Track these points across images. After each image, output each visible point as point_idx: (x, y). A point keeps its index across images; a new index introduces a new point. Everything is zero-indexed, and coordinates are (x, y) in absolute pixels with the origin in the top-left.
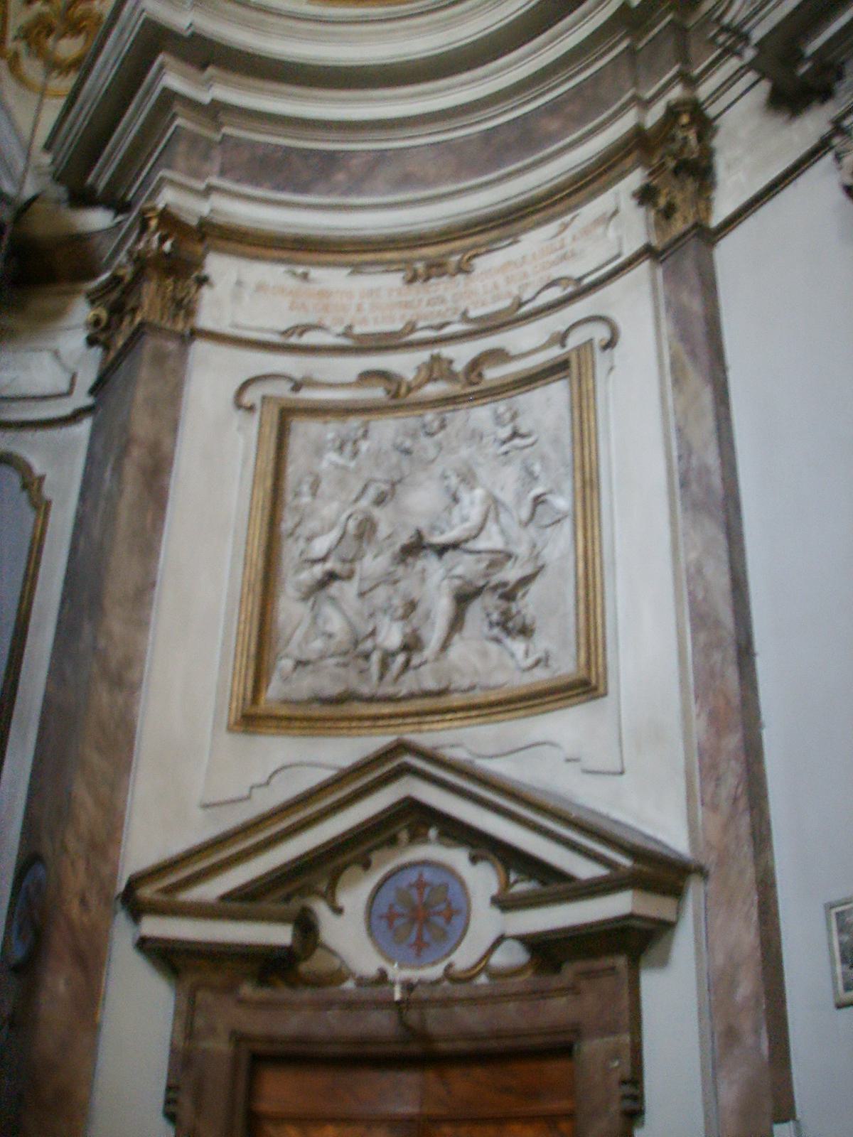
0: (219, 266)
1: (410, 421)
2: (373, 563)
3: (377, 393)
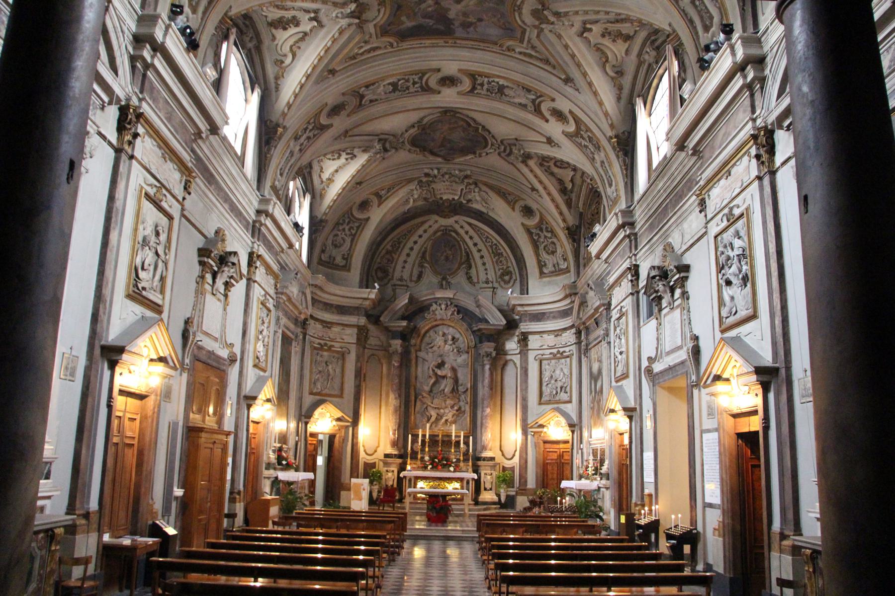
0: (530, 337)
1: (557, 361)
2: (553, 382)
3: (551, 356)
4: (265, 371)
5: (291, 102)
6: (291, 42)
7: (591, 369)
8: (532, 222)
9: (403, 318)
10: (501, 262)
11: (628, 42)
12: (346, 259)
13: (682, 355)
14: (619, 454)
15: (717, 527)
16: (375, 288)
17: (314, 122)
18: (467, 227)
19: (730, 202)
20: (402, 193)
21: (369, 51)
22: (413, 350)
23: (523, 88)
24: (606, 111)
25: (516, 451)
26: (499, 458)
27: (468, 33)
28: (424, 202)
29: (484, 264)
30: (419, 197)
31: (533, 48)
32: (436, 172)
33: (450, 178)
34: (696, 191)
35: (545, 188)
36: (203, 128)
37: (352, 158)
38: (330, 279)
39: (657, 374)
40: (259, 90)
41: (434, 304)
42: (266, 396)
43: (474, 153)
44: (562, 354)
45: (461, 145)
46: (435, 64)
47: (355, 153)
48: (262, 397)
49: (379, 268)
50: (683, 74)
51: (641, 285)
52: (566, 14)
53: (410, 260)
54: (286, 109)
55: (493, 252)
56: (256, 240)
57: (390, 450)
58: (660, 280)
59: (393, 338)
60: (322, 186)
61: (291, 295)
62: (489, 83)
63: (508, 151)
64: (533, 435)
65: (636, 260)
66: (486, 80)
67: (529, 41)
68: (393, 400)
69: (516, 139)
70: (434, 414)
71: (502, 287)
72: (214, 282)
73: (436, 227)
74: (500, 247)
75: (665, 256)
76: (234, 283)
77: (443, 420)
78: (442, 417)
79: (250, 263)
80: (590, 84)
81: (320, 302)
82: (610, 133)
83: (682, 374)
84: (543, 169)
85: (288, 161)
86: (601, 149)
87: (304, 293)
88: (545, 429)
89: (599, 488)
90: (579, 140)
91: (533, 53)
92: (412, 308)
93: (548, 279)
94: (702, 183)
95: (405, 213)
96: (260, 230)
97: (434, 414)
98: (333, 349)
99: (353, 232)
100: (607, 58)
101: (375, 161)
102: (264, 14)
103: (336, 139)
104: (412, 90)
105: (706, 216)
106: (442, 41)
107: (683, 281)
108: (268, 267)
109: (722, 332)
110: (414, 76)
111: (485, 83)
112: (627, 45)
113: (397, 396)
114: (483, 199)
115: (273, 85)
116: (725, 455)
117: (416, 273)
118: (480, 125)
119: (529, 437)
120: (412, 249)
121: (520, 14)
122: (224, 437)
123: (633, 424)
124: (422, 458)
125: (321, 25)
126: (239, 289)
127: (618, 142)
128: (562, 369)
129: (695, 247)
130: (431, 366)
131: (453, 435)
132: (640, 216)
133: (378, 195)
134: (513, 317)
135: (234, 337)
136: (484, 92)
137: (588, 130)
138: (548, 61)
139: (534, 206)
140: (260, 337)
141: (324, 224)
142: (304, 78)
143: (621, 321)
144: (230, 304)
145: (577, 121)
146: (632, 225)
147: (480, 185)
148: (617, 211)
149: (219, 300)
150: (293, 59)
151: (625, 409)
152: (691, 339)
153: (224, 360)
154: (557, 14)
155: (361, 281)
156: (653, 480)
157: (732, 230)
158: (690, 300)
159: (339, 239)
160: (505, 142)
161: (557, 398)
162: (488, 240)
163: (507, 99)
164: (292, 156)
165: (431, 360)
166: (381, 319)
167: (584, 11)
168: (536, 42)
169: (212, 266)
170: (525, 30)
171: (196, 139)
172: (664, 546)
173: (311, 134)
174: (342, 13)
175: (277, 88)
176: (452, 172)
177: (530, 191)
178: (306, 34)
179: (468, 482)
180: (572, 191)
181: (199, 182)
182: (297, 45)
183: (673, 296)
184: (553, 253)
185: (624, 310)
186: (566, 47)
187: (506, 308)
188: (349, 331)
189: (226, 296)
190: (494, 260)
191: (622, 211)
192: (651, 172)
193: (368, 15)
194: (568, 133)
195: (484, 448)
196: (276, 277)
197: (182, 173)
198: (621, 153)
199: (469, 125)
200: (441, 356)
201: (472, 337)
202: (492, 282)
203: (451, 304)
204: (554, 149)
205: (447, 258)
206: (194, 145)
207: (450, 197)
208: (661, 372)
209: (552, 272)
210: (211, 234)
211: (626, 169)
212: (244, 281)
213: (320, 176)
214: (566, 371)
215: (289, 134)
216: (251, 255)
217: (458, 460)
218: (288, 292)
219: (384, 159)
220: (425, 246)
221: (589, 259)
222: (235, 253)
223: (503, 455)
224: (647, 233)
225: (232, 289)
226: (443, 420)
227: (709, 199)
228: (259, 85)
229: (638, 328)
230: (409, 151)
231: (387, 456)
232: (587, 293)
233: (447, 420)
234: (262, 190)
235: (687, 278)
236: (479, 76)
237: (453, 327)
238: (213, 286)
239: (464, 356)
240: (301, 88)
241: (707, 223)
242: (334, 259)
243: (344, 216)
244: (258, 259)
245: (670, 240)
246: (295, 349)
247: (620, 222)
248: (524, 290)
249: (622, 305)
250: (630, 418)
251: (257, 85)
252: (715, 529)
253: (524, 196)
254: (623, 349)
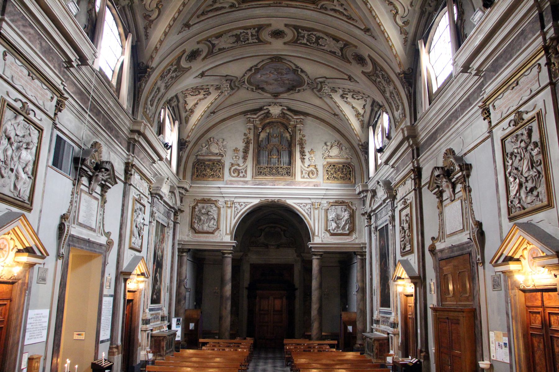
4: (140, 251)
36: (73, 58)
37: (208, 95)
47: (210, 91)
48: (137, 271)
135: (112, 226)
173: (174, 75)
183: (454, 191)
185: (408, 202)
191: (407, 127)
225: (109, 191)
235: (468, 176)
244: (132, 168)
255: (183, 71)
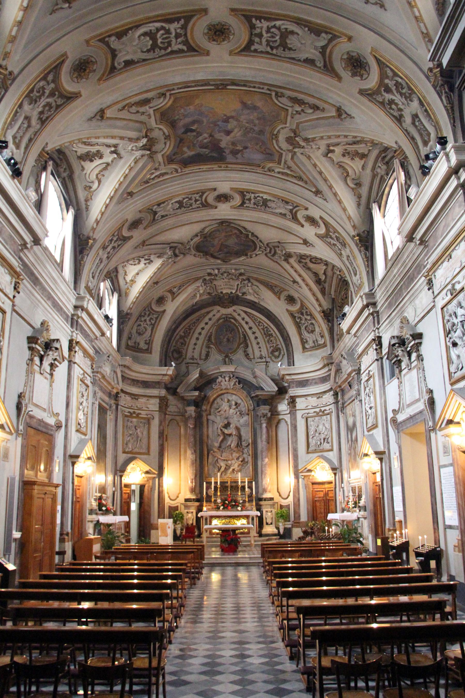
0: (298, 400)
2: (317, 435)
3: (315, 414)
4: (85, 435)
5: (99, 218)
6: (96, 171)
7: (347, 423)
8: (295, 308)
9: (195, 389)
10: (271, 341)
11: (364, 159)
12: (148, 344)
13: (421, 406)
14: (373, 490)
15: (457, 545)
16: (172, 366)
17: (118, 235)
18: (243, 315)
19: (452, 280)
20: (190, 290)
21: (158, 176)
22: (204, 414)
23: (283, 200)
24: (349, 215)
25: (290, 492)
26: (277, 499)
27: (237, 158)
28: (208, 296)
29: (258, 343)
30: (204, 292)
31: (289, 168)
32: (216, 271)
33: (228, 276)
34: (424, 273)
35: (304, 280)
37: (149, 263)
38: (136, 360)
39: (401, 423)
40: (73, 210)
41: (220, 377)
42: (87, 455)
43: (246, 255)
44: (323, 412)
45: (235, 249)
46: (212, 185)
47: (152, 259)
48: (84, 455)
49: (174, 350)
50: (408, 182)
51: (384, 353)
52: (313, 140)
53: (200, 342)
54: (95, 224)
55: (265, 334)
56: (74, 329)
57: (190, 496)
58: (399, 347)
59: (189, 405)
60: (126, 287)
61: (105, 374)
62: (255, 198)
63: (273, 252)
64: (304, 479)
65: (379, 333)
66: (253, 195)
67: (285, 163)
68: (190, 455)
69: (279, 242)
70: (223, 464)
71: (273, 361)
72: (41, 363)
73: (218, 316)
74: (270, 329)
75: (402, 328)
76: (58, 364)
77: (231, 470)
78: (229, 467)
79: (71, 348)
80: (335, 194)
81: (128, 378)
82: (353, 233)
83: (421, 421)
84: (301, 265)
85: (98, 266)
86: (347, 246)
87: (115, 372)
88: (313, 473)
89: (359, 518)
90: (329, 240)
91: (289, 172)
92: (203, 381)
93: (309, 353)
94: (428, 266)
95: (193, 306)
96: (77, 321)
97: (223, 464)
98: (140, 416)
99: (153, 322)
100: (348, 173)
101: (168, 265)
102: (74, 149)
103: (136, 248)
104: (194, 206)
105: (433, 292)
106: (216, 166)
107: (418, 347)
108: (85, 352)
109: (452, 384)
110: (195, 195)
111: (252, 198)
112: (363, 162)
113: (193, 451)
114: (255, 292)
115: (84, 206)
116: (460, 485)
117: (204, 353)
118: (250, 232)
119: (300, 480)
120: (200, 334)
121: (277, 141)
122: (53, 489)
123: (383, 464)
124: (215, 501)
125: (121, 158)
126: (62, 368)
127: (360, 240)
128: (324, 424)
129: (426, 318)
130: (220, 426)
131: (240, 481)
132: (380, 297)
133: (170, 291)
134: (283, 385)
135: (60, 408)
136: (252, 205)
137: (336, 231)
138: (301, 178)
139: (296, 295)
140: (81, 407)
141: (129, 316)
142: (109, 200)
143: (369, 382)
144: (55, 382)
145: (326, 224)
146: (374, 304)
147: (252, 280)
148: (362, 294)
149: (46, 378)
150: (99, 184)
151: (376, 453)
152: (427, 392)
153: (52, 426)
154: (306, 140)
155: (161, 361)
156: (401, 509)
157: (455, 302)
158: (424, 362)
159: (142, 328)
160: (270, 245)
161: (321, 448)
162: (260, 324)
163: (270, 210)
164: (101, 262)
165: (219, 422)
166: (178, 390)
167: (328, 136)
168: (290, 163)
169: (39, 351)
170: (282, 154)
171: (22, 249)
172: (414, 563)
173: (116, 245)
174: (136, 146)
175: (87, 209)
176: (230, 271)
177: (292, 283)
178: (108, 164)
179: (253, 519)
180: (325, 282)
181: (26, 284)
182: (102, 173)
183: (410, 359)
184: (313, 332)
185: (371, 373)
186: (315, 166)
187: (277, 378)
188: (153, 401)
189: (52, 375)
190: (266, 340)
192: (388, 261)
193: (158, 147)
194: (319, 234)
195: (265, 491)
196: (92, 359)
197: (12, 276)
198: (362, 249)
199: (241, 233)
200: (227, 418)
201: (251, 402)
202: (265, 358)
203: (233, 376)
204: (308, 249)
205: (228, 340)
206: (22, 254)
207: (229, 291)
208: (404, 421)
209: (313, 347)
210: (37, 325)
211: (367, 261)
212: (66, 363)
213: (124, 278)
214: (327, 425)
215: (97, 245)
216: (71, 341)
217: (244, 502)
218: (102, 371)
219: (175, 262)
220: (211, 331)
221: (341, 335)
222: (58, 340)
223: (280, 495)
224: (386, 310)
225: (57, 369)
226: (231, 470)
227: (435, 278)
228: (73, 206)
229: (383, 386)
230: (195, 255)
231: (186, 500)
232: (341, 362)
233: (233, 470)
234: (78, 290)
235: (421, 343)
236: (247, 192)
237: (235, 395)
238: (40, 367)
239: (246, 418)
240: (106, 207)
241: (434, 298)
242: (139, 344)
243: (145, 310)
244: (76, 345)
245: (405, 314)
246: (110, 416)
247: (365, 303)
248: (291, 363)
249: (369, 369)
250: (381, 460)
251: (71, 207)
252: (455, 546)
253: (287, 288)
254: (372, 405)
255: (124, 241)
